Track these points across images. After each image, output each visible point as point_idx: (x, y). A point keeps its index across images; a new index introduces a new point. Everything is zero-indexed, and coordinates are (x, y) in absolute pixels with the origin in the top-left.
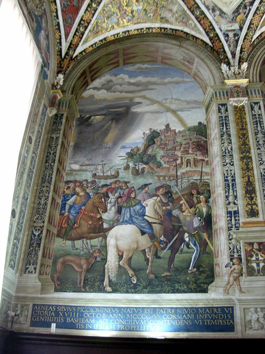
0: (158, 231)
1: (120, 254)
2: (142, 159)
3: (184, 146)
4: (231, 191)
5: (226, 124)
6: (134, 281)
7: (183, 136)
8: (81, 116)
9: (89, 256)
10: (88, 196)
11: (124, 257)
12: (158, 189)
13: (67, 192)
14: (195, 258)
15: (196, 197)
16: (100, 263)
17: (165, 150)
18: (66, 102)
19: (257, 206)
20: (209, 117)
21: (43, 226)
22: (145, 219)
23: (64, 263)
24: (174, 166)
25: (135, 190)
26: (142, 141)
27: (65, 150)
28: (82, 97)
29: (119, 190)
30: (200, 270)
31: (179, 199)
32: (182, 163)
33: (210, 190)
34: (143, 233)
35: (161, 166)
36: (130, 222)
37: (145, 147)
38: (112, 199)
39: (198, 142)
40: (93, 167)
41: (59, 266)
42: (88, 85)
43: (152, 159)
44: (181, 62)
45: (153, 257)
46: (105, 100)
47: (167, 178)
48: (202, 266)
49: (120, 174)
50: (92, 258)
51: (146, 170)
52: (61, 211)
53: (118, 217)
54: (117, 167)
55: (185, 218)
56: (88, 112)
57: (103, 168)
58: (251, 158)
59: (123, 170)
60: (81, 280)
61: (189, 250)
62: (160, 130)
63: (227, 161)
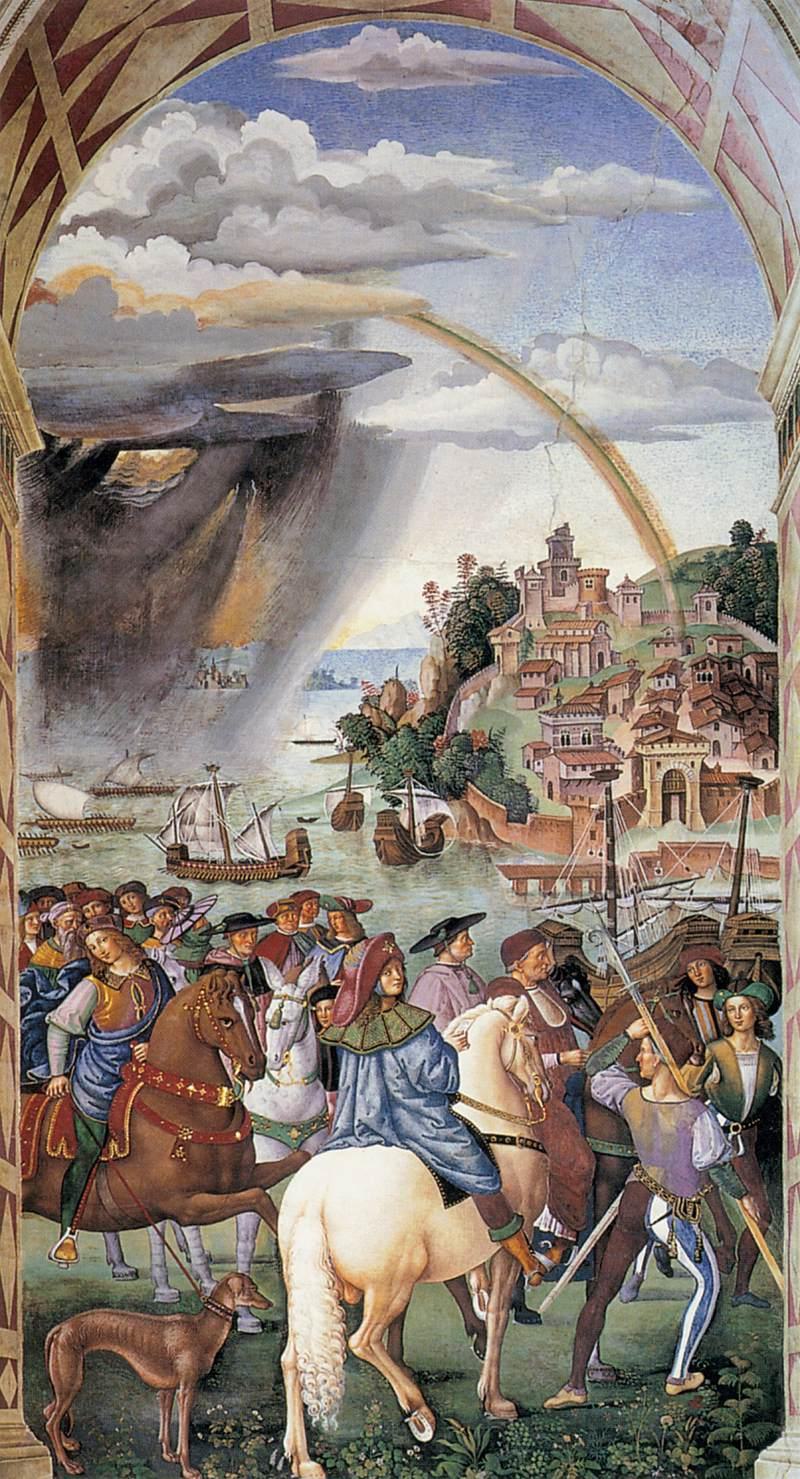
0: (524, 1183)
1: (348, 1297)
2: (427, 757)
3: (652, 684)
6: (422, 1429)
8: (49, 439)
9: (198, 1309)
10: (163, 988)
11: (368, 1311)
12: (513, 949)
13: (40, 954)
14: (696, 1325)
15: (710, 1003)
16: (255, 1346)
17: (551, 705)
23: (79, 1346)
25: (399, 957)
28: (39, 294)
29: (320, 953)
30: (721, 1381)
31: (624, 1010)
32: (639, 798)
34: (452, 1193)
36: (386, 1131)
37: (437, 682)
38: (287, 1003)
39: (730, 662)
40: (165, 801)
41: (58, 1362)
42: (60, 193)
43: (483, 766)
45: (502, 1314)
46: (179, 325)
47: (560, 886)
49: (317, 857)
50: (213, 1322)
51: (452, 838)
52: (27, 1064)
54: (299, 813)
55: (655, 1117)
56: (96, 414)
60: (173, 1428)
61: (673, 1284)
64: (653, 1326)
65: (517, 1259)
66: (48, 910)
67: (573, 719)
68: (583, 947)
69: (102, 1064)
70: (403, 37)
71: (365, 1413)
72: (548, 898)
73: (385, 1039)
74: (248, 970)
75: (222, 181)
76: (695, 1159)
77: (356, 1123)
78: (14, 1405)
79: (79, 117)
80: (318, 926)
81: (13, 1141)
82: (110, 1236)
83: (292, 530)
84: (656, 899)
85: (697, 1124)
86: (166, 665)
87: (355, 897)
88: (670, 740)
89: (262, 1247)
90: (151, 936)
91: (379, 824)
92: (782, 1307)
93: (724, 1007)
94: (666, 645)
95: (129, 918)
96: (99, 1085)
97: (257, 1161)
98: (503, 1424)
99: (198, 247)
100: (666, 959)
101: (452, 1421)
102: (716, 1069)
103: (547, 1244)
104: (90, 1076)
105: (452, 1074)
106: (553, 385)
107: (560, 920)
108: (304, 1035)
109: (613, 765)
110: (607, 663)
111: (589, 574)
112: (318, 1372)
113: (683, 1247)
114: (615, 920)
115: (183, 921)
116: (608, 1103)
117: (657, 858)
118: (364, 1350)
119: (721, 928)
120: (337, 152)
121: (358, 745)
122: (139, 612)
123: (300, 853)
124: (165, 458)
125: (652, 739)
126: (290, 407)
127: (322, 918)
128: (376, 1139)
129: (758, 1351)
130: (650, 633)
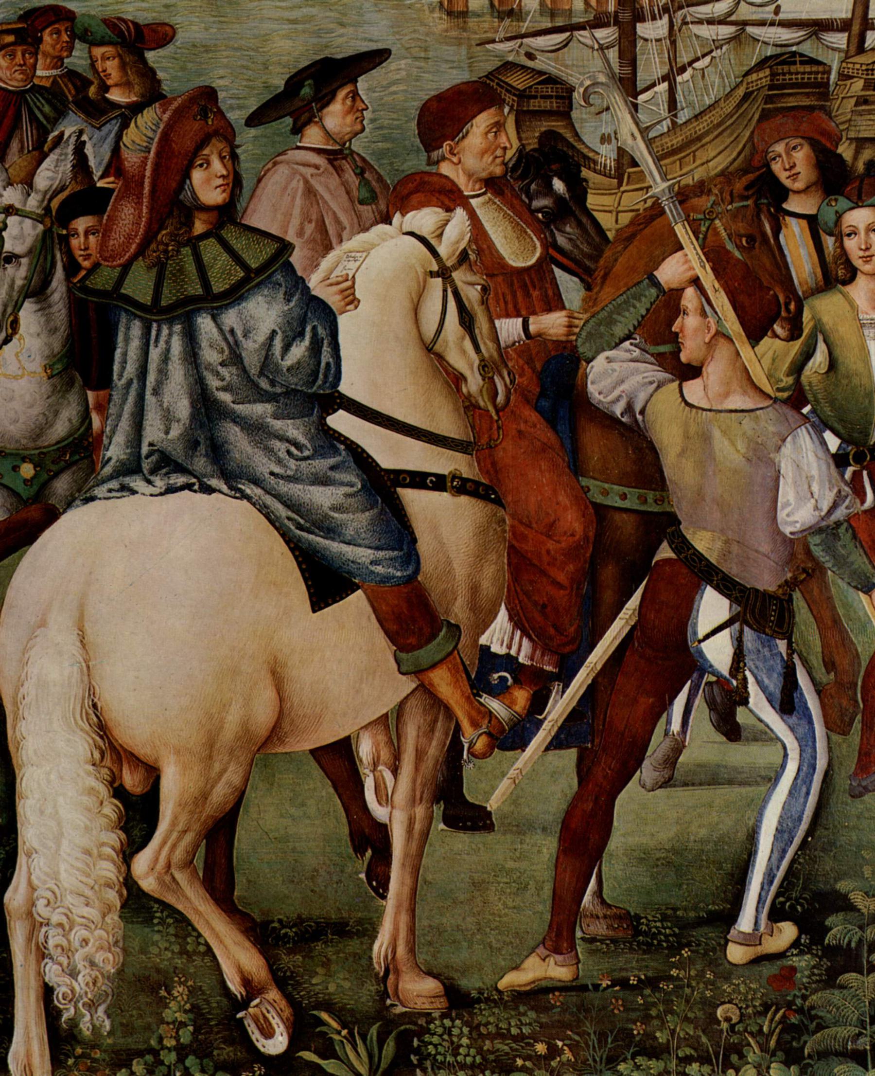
1: (131, 780)
6: (268, 1033)
14: (783, 833)
15: (812, 221)
29: (69, 127)
36: (201, 464)
45: (420, 811)
48: (843, 904)
53: (86, 417)
55: (706, 438)
64: (703, 832)
65: (449, 713)
68: (574, 114)
72: (507, 22)
76: (781, 515)
77: (145, 450)
80: (72, 75)
84: (711, 22)
85: (787, 449)
98: (422, 1021)
101: (324, 1016)
102: (821, 348)
103: (503, 679)
105: (326, 356)
107: (530, 64)
108: (46, 282)
113: (759, 682)
114: (633, 63)
116: (618, 410)
119: (833, 76)
128: (180, 480)
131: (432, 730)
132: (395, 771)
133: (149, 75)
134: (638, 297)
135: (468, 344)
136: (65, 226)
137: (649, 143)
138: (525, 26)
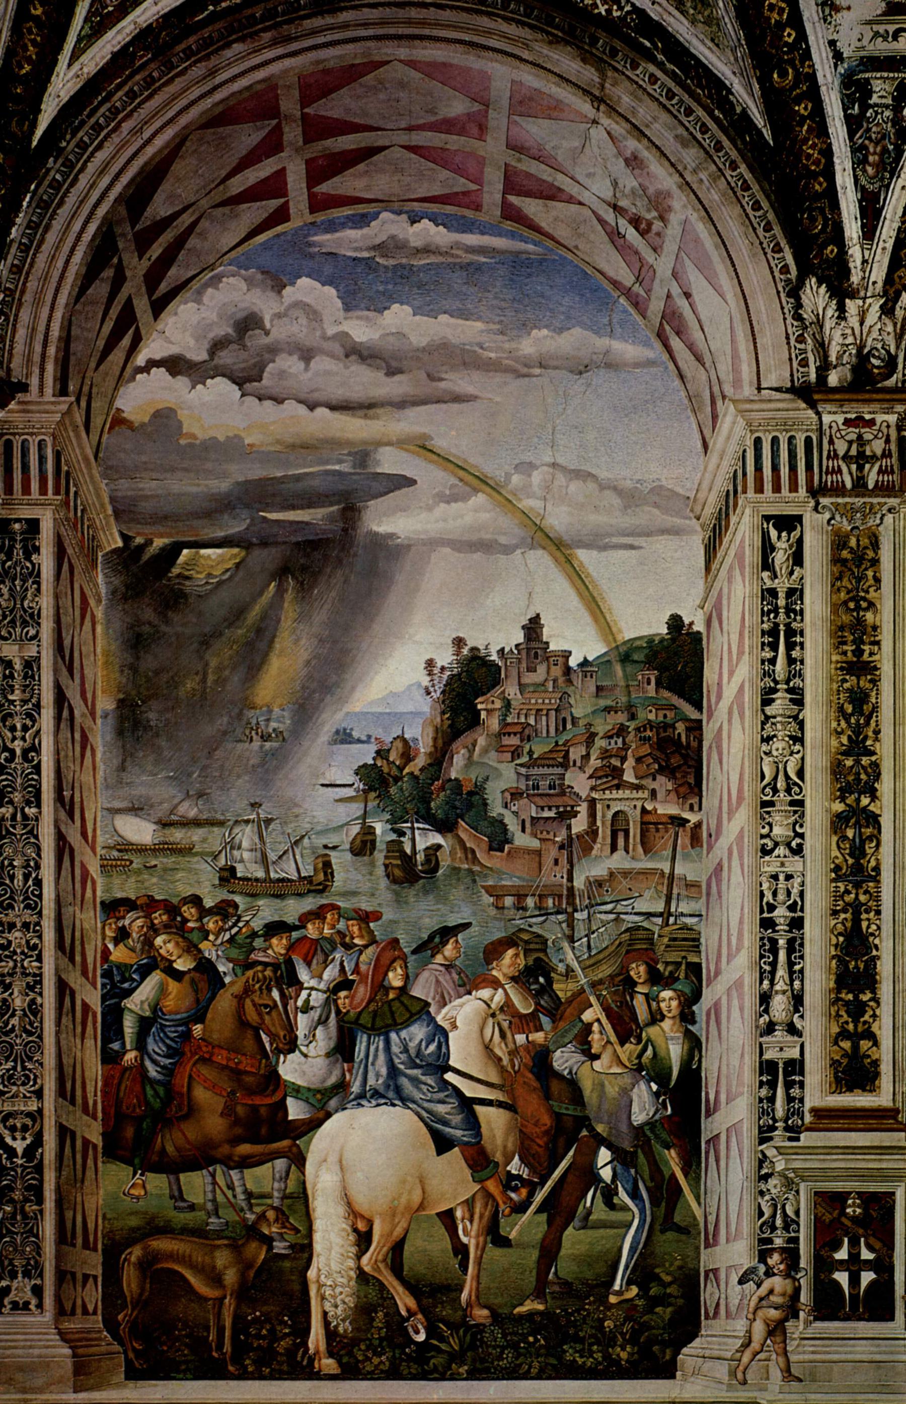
1: (361, 1226)
2: (425, 798)
4: (781, 972)
5: (790, 633)
7: (599, 689)
8: (126, 538)
10: (216, 981)
12: (493, 952)
13: (119, 954)
14: (633, 1249)
15: (647, 995)
16: (287, 1264)
17: (525, 759)
18: (41, 445)
19: (876, 1044)
20: (714, 593)
21: (40, 1111)
22: (447, 1083)
23: (146, 1265)
24: (562, 847)
26: (425, 706)
27: (77, 736)
28: (119, 421)
30: (652, 1292)
31: (579, 1001)
32: (592, 832)
33: (699, 966)
34: (443, 1144)
35: (508, 841)
36: (391, 1094)
37: (435, 739)
39: (666, 726)
41: (130, 1280)
42: (137, 340)
43: (470, 806)
44: (601, 221)
45: (481, 1239)
47: (530, 902)
48: (657, 1278)
51: (445, 861)
52: (106, 1041)
53: (344, 1075)
54: (325, 841)
55: (602, 1085)
57: (261, 837)
58: (874, 820)
59: (349, 856)
62: (501, 651)
63: (777, 831)
65: (494, 1200)
66: (124, 917)
67: (542, 771)
69: (168, 1041)
70: (413, 222)
71: (373, 1319)
73: (390, 1022)
74: (283, 966)
75: (267, 333)
76: (633, 1117)
78: (95, 1313)
79: (153, 278)
80: (339, 932)
81: (95, 1103)
82: (172, 1177)
83: (320, 616)
84: (606, 913)
85: (635, 1090)
86: (219, 722)
87: (369, 909)
88: (618, 787)
89: (292, 1186)
90: (206, 938)
91: (388, 851)
92: (699, 1233)
93: (657, 999)
94: (616, 712)
95: (190, 924)
96: (164, 1056)
97: (290, 1118)
99: (247, 386)
100: (612, 961)
102: (650, 1048)
104: (157, 1050)
105: (444, 1050)
106: (529, 503)
108: (327, 1018)
109: (572, 807)
110: (569, 726)
111: (555, 654)
112: (336, 1285)
114: (573, 930)
115: (231, 928)
116: (566, 1073)
117: (605, 880)
118: (373, 1268)
120: (360, 313)
121: (371, 789)
122: (197, 679)
123: (326, 874)
124: (220, 555)
125: (603, 787)
126: (319, 516)
127: (341, 926)
128: (383, 1101)
129: (680, 1268)
130: (603, 703)
131: (487, 1205)
132: (471, 1221)
133: (371, 932)
134: (574, 1026)
135: (503, 1045)
136: (335, 994)
137: (579, 962)
138: (528, 914)
